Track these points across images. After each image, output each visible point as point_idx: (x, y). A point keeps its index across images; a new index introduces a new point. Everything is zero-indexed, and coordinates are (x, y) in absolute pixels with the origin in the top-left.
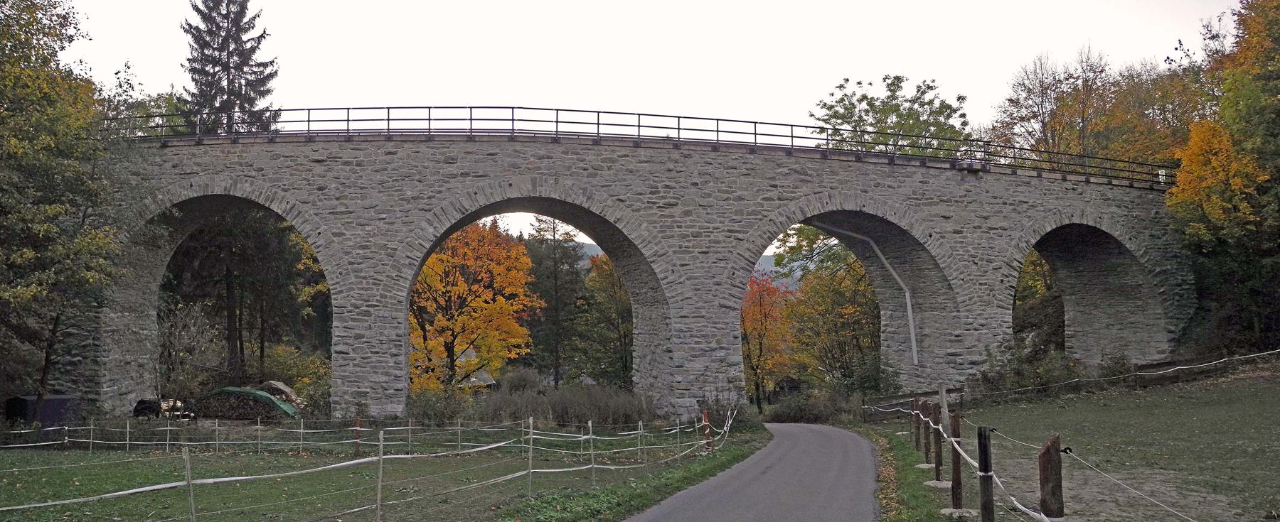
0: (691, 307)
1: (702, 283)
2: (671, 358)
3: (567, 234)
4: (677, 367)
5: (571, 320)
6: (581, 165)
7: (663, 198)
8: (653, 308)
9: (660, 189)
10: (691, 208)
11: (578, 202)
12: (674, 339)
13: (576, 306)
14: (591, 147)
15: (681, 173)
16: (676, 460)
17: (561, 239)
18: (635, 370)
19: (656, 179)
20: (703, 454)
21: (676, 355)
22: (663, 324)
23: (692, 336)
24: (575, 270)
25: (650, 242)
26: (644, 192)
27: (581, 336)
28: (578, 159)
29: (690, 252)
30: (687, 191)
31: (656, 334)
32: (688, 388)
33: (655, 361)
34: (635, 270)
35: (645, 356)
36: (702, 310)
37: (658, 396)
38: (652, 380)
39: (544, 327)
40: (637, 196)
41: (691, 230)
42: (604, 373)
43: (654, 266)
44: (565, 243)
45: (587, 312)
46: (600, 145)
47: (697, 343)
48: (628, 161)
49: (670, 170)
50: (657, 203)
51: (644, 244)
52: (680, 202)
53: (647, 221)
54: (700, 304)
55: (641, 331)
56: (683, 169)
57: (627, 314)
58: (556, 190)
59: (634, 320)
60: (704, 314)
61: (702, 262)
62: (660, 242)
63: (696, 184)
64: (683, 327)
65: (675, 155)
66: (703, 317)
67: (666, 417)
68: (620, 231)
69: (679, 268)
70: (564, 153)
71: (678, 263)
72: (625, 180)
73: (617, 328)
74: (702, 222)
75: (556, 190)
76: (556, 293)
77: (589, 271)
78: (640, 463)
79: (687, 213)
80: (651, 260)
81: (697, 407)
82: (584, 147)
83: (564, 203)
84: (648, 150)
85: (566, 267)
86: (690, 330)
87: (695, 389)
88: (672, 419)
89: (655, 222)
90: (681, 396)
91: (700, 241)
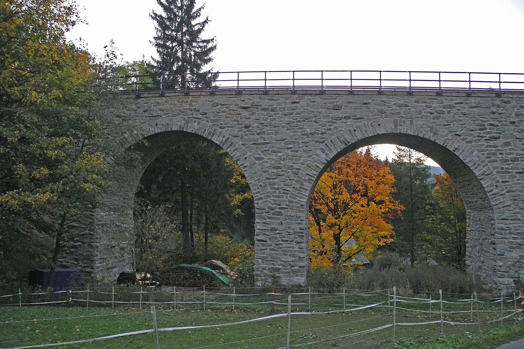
0: (510, 212)
1: (519, 195)
2: (495, 249)
3: (419, 159)
4: (499, 255)
5: (422, 219)
6: (429, 110)
7: (489, 133)
8: (481, 212)
9: (486, 127)
10: (509, 140)
11: (427, 137)
12: (497, 235)
13: (425, 210)
14: (435, 97)
15: (502, 115)
16: (500, 322)
17: (415, 162)
18: (468, 256)
19: (484, 119)
20: (519, 319)
21: (499, 246)
22: (489, 224)
23: (510, 233)
24: (424, 185)
25: (479, 165)
26: (474, 129)
27: (428, 231)
28: (426, 106)
29: (509, 173)
30: (507, 128)
31: (483, 231)
32: (507, 271)
33: (483, 250)
34: (468, 185)
35: (475, 246)
36: (518, 215)
37: (484, 275)
38: (480, 264)
39: (403, 224)
40: (469, 132)
41: (509, 156)
42: (445, 257)
43: (483, 182)
44: (418, 165)
45: (433, 214)
46: (442, 96)
47: (514, 238)
48: (462, 107)
49: (493, 113)
50: (483, 137)
51: (475, 167)
52: (501, 136)
53: (478, 150)
54: (517, 210)
55: (472, 228)
56: (503, 112)
57: (462, 217)
58: (411, 129)
59: (467, 221)
60: (520, 217)
61: (519, 180)
62: (487, 165)
63: (514, 123)
64: (504, 226)
65: (497, 102)
66: (519, 220)
67: (490, 291)
68: (458, 157)
69: (501, 184)
70: (415, 102)
71: (501, 180)
72: (460, 120)
73: (454, 226)
74: (518, 150)
75: (411, 129)
76: (412, 200)
77: (434, 185)
78: (473, 322)
79: (507, 144)
80: (480, 178)
81: (513, 285)
82: (430, 97)
83: (417, 137)
84: (476, 98)
85: (418, 182)
86: (509, 229)
87: (512, 272)
88: (494, 292)
89: (483, 150)
90: (501, 276)
91: (517, 164)
